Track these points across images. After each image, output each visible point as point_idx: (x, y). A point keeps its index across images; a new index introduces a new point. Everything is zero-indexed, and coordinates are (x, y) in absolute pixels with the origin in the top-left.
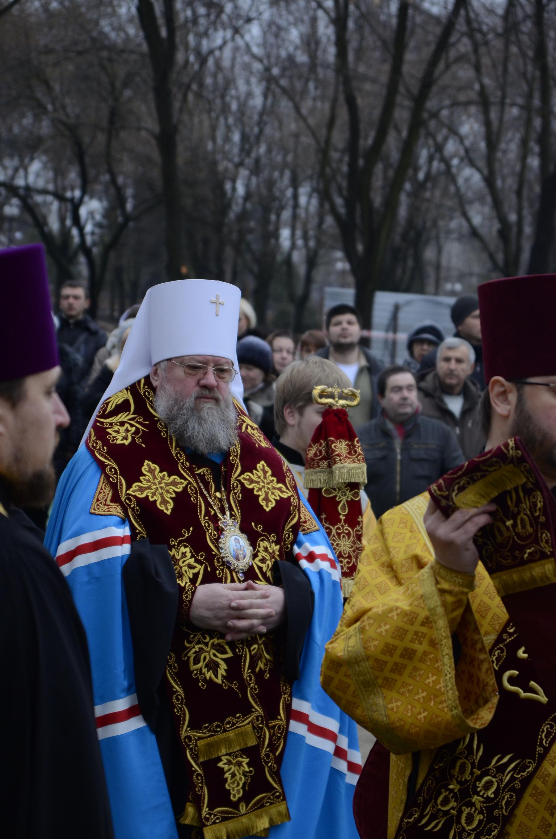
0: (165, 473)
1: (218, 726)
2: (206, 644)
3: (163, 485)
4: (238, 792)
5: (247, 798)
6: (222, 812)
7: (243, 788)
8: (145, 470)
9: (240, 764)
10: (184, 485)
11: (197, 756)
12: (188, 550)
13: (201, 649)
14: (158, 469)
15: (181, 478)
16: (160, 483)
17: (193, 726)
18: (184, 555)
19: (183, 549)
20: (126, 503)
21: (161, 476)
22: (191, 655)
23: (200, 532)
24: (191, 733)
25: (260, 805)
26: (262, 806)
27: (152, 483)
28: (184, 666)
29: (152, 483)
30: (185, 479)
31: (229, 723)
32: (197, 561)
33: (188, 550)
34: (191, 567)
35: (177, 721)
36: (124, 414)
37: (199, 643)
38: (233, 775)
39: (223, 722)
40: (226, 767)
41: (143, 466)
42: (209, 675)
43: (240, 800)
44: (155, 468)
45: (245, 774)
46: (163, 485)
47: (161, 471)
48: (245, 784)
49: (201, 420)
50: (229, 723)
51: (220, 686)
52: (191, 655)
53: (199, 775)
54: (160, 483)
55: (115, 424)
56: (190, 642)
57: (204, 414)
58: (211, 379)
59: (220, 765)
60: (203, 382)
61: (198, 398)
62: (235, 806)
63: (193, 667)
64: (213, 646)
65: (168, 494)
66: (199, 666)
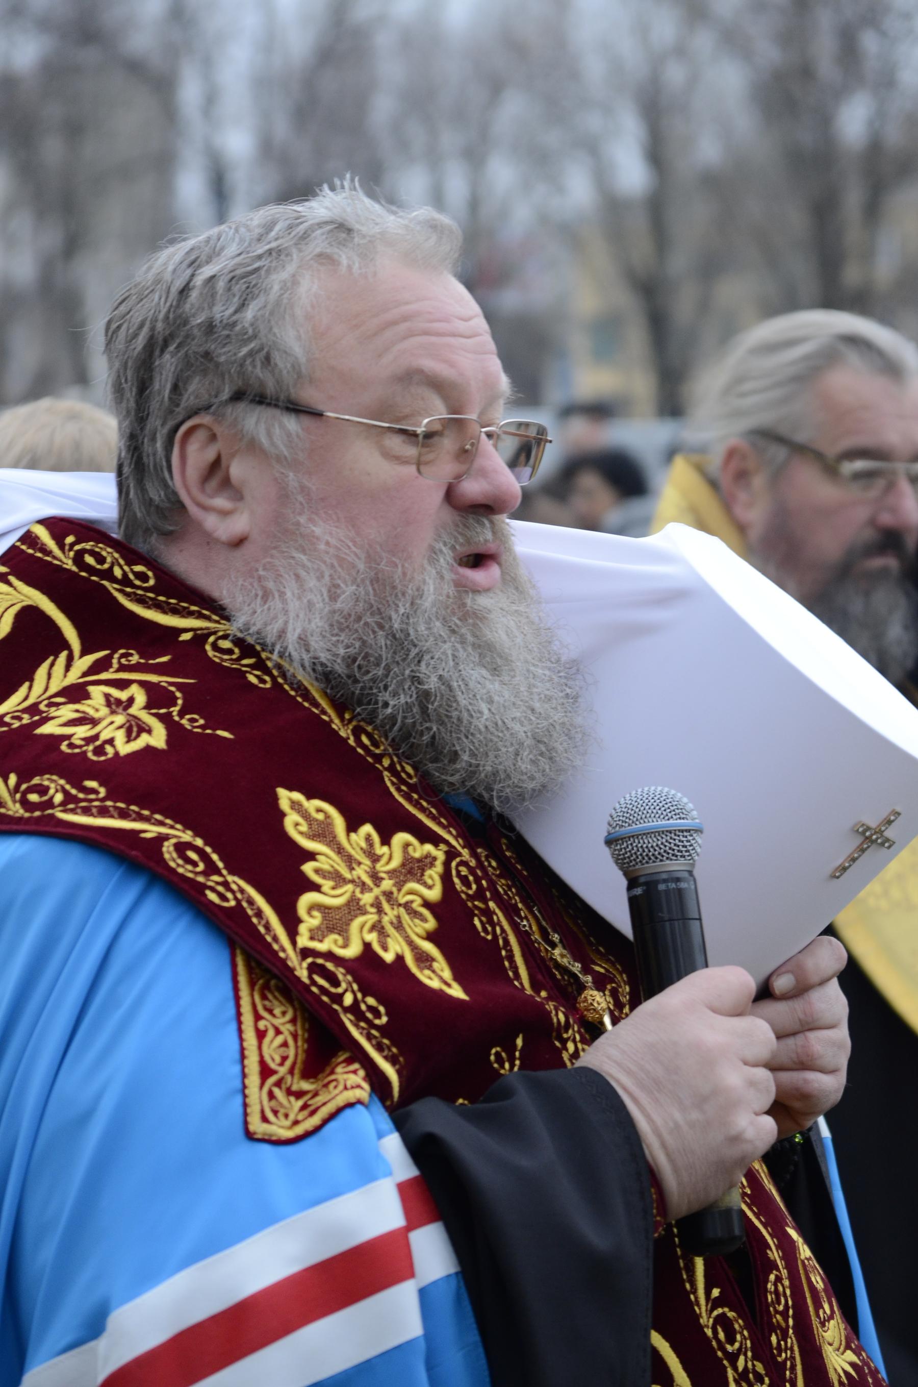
0: (367, 829)
3: (387, 884)
8: (301, 833)
10: (439, 867)
14: (339, 822)
15: (422, 841)
16: (376, 878)
20: (321, 988)
21: (363, 844)
27: (352, 881)
29: (352, 881)
30: (436, 840)
36: (52, 665)
41: (283, 815)
44: (327, 816)
46: (387, 884)
47: (352, 827)
54: (376, 878)
55: (50, 705)
65: (417, 921)
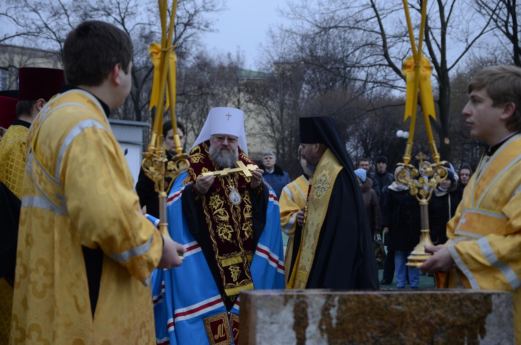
1: (228, 255)
2: (224, 227)
4: (236, 278)
5: (239, 280)
6: (230, 285)
7: (237, 277)
9: (236, 269)
11: (221, 265)
12: (218, 196)
13: (223, 229)
17: (220, 255)
18: (217, 198)
19: (216, 196)
22: (219, 231)
23: (223, 190)
24: (220, 257)
25: (244, 284)
26: (244, 284)
28: (217, 234)
31: (232, 254)
32: (221, 200)
33: (218, 196)
34: (219, 202)
35: (215, 253)
37: (222, 226)
38: (234, 273)
39: (230, 254)
40: (231, 270)
42: (225, 237)
43: (236, 281)
45: (238, 272)
48: (238, 276)
49: (222, 156)
50: (232, 254)
51: (229, 241)
52: (219, 231)
53: (222, 272)
56: (219, 226)
57: (223, 154)
58: (226, 142)
59: (229, 269)
60: (223, 144)
61: (221, 149)
62: (235, 283)
63: (220, 235)
64: (227, 228)
66: (221, 234)
